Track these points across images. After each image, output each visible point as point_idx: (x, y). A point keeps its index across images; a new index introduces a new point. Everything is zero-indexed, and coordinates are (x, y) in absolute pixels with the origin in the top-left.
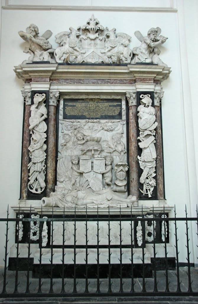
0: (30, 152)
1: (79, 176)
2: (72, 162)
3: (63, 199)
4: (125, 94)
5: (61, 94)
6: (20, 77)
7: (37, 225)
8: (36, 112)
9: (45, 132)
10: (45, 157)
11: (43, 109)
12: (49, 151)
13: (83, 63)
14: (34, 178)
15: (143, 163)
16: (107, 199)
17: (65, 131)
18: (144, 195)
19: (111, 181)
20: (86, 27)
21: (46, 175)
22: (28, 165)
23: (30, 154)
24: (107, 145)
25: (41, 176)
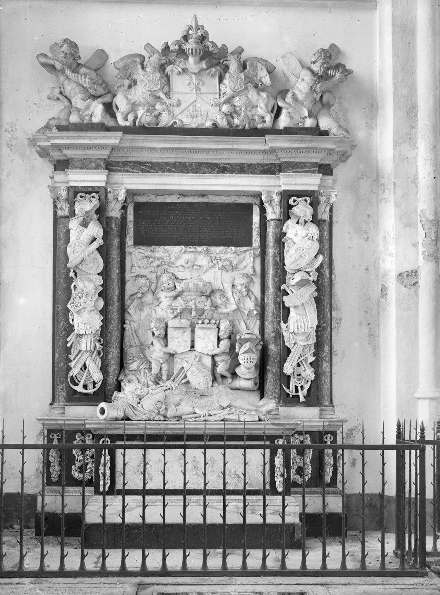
0: (70, 313)
3: (138, 406)
4: (259, 195)
5: (131, 193)
6: (43, 154)
8: (81, 232)
9: (99, 274)
11: (95, 229)
13: (175, 126)
14: (80, 365)
17: (138, 269)
18: (291, 396)
20: (180, 46)
21: (104, 359)
22: (68, 339)
23: (70, 316)
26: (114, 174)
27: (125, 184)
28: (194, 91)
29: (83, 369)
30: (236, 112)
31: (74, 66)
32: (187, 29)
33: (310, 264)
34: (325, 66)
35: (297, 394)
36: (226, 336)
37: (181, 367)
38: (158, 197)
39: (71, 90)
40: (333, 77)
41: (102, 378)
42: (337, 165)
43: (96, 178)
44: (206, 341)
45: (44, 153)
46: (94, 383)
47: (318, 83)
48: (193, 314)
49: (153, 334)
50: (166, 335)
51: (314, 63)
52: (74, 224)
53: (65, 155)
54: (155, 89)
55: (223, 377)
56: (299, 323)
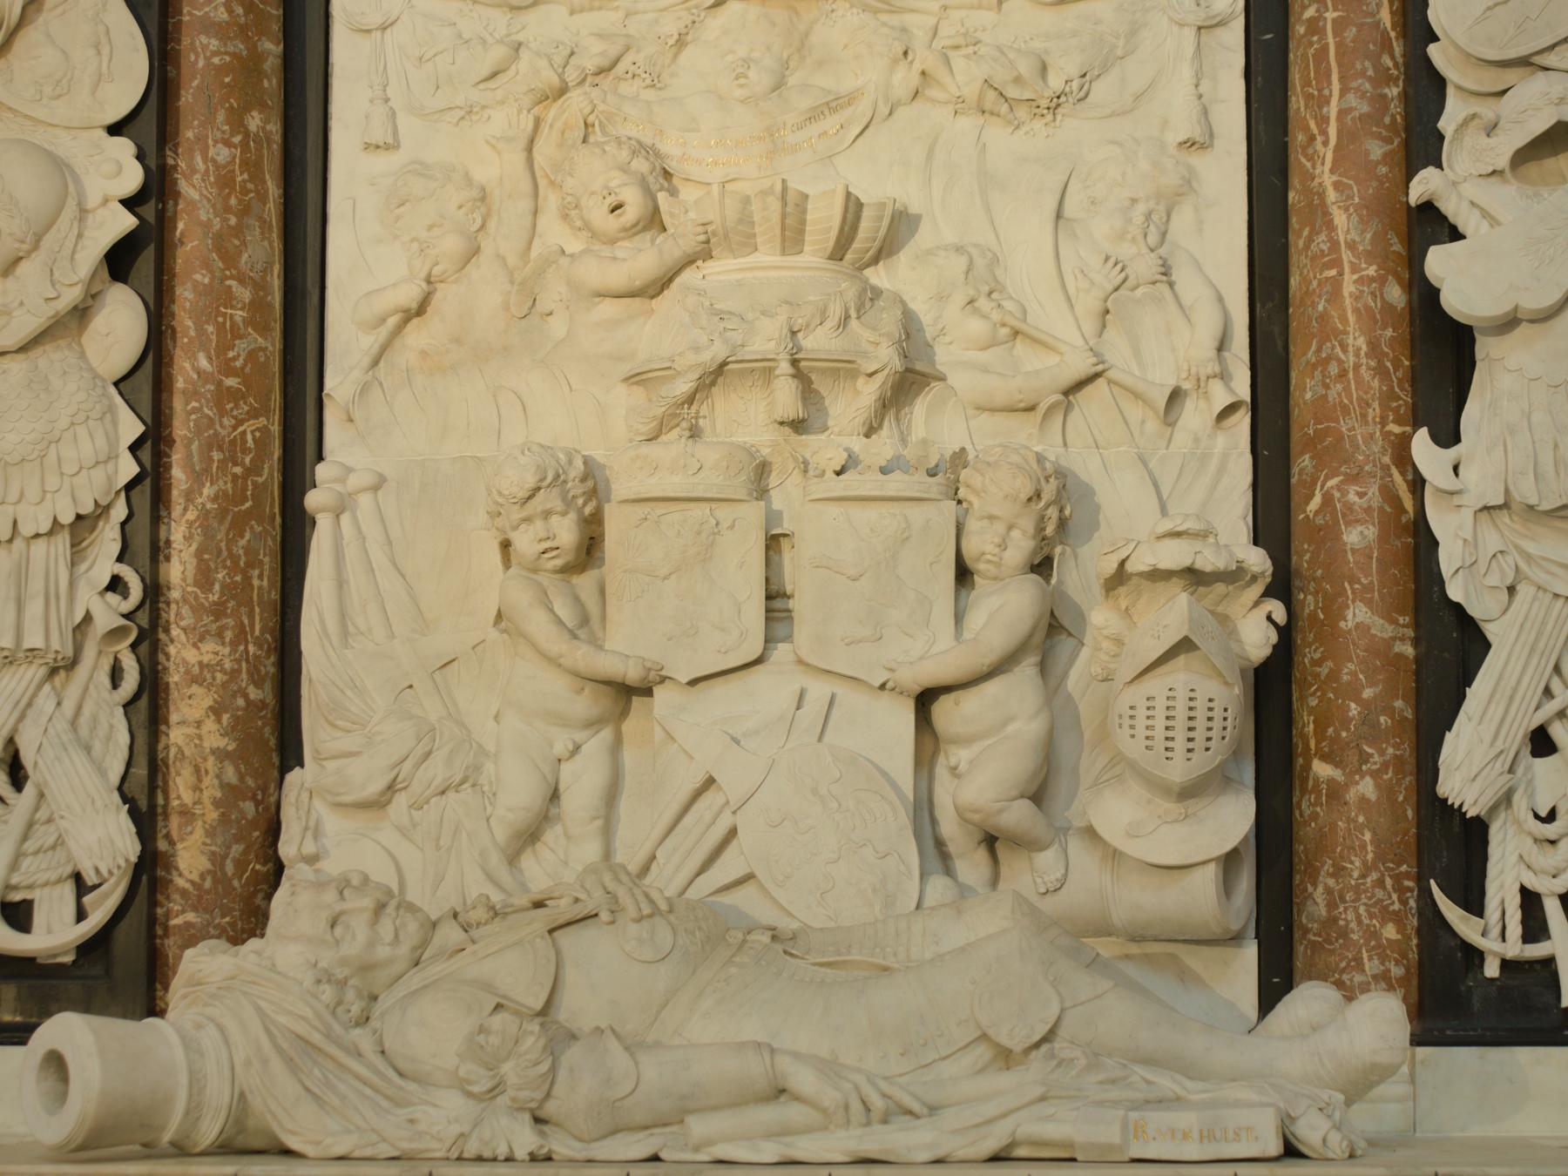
1: (594, 724)
2: (506, 545)
9: (115, 130)
10: (128, 468)
12: (180, 383)
15: (1491, 540)
16: (984, 1037)
19: (1038, 795)
24: (983, 303)
25: (74, 723)
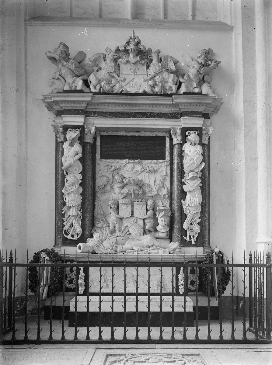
0: (64, 195)
4: (169, 131)
6: (50, 109)
7: (73, 273)
8: (70, 149)
9: (80, 173)
11: (77, 147)
13: (122, 92)
17: (102, 172)
18: (187, 242)
20: (125, 48)
21: (83, 220)
23: (64, 197)
26: (90, 118)
27: (95, 124)
28: (133, 73)
29: (71, 226)
30: (156, 84)
31: (67, 59)
32: (129, 38)
33: (197, 168)
34: (206, 59)
35: (191, 240)
36: (150, 209)
37: (126, 225)
38: (113, 133)
39: (65, 73)
40: (209, 65)
41: (82, 231)
42: (212, 114)
43: (79, 120)
44: (140, 211)
45: (50, 107)
46: (77, 234)
47: (202, 68)
48: (133, 196)
49: (111, 208)
50: (118, 208)
51: (199, 57)
52: (66, 145)
53: (61, 107)
54: (111, 72)
55: (150, 231)
56: (192, 200)
